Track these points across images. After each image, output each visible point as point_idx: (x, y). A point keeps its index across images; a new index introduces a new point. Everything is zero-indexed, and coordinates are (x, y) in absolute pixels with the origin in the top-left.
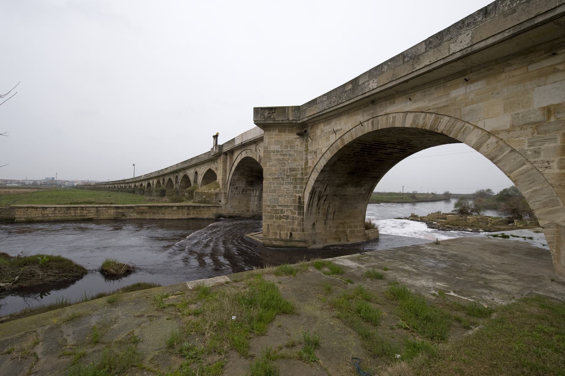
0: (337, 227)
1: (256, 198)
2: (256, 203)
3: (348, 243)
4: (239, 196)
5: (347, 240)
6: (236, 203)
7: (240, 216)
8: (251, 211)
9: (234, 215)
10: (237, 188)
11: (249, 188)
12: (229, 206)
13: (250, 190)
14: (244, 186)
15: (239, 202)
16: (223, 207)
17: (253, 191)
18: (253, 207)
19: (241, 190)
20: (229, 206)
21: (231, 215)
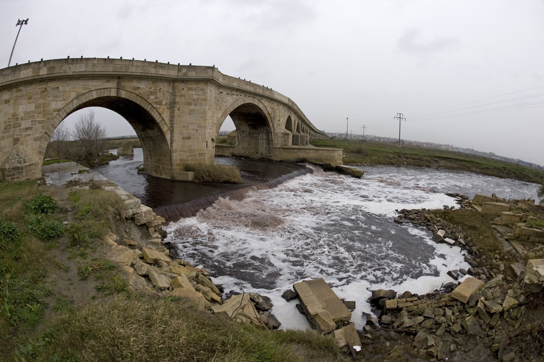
0: (156, 162)
1: (264, 141)
2: (265, 146)
3: (161, 177)
4: (247, 139)
5: (161, 175)
6: (246, 145)
7: (249, 157)
8: (260, 153)
9: (243, 155)
10: (243, 132)
11: (254, 131)
12: (240, 147)
13: (255, 133)
14: (248, 129)
15: (249, 145)
16: (236, 148)
17: (259, 134)
18: (262, 149)
19: (247, 133)
20: (240, 147)
21: (241, 155)
